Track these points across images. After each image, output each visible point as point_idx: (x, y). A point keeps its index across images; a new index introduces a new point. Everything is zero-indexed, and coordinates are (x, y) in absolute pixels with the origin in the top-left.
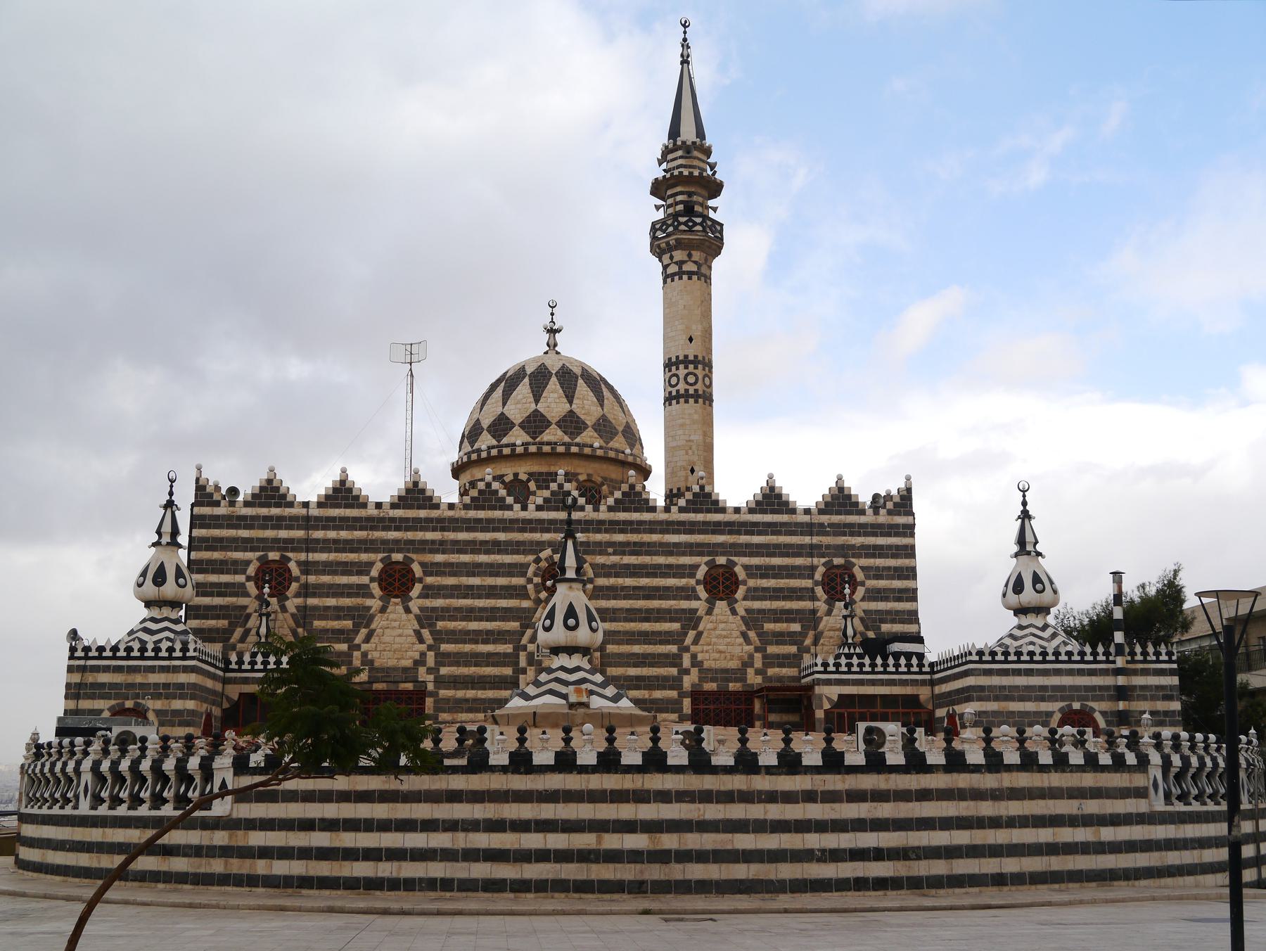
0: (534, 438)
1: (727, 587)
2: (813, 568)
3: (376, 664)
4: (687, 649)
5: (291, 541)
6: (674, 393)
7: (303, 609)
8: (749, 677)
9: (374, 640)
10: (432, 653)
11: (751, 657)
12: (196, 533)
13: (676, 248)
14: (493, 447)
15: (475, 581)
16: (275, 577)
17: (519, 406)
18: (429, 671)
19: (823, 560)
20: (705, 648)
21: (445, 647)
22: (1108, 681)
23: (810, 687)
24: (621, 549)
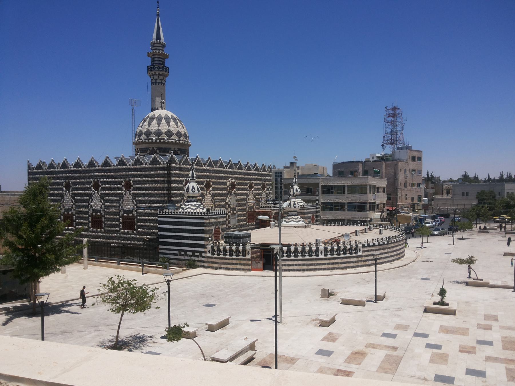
13: (161, 75)
22: (315, 210)
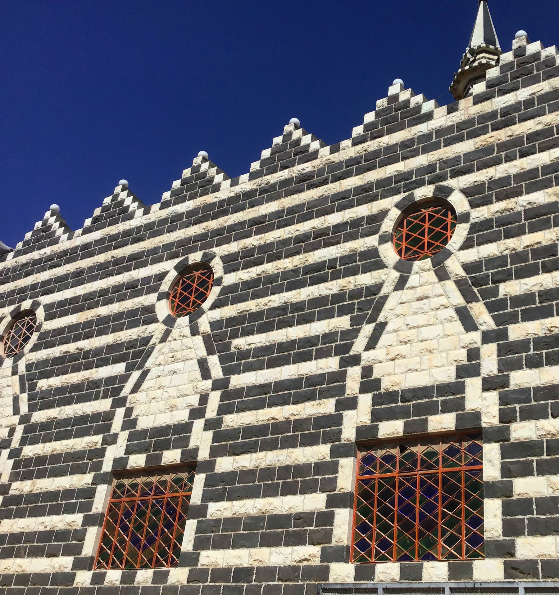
3: (386, 384)
9: (384, 339)
18: (489, 385)
21: (517, 332)
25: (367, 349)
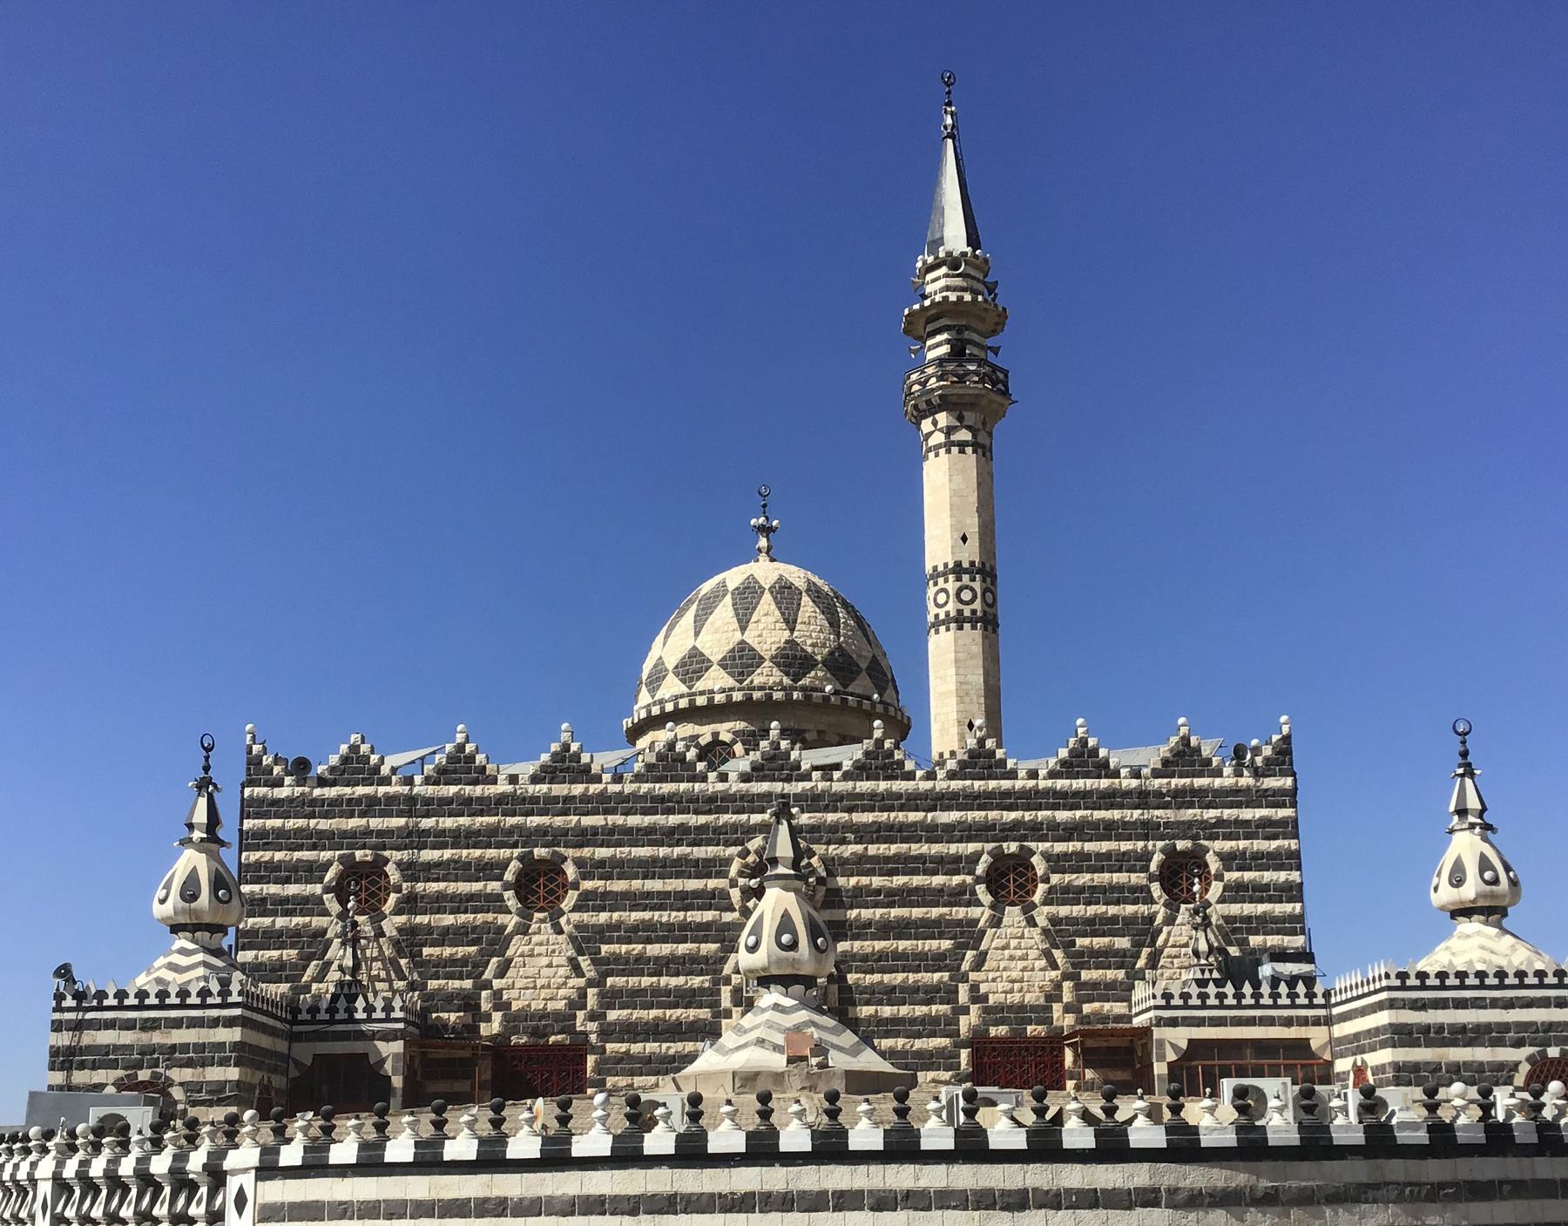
0: (741, 682)
1: (1021, 887)
2: (1146, 856)
4: (964, 978)
5: (388, 833)
6: (942, 617)
7: (409, 932)
8: (1055, 1015)
10: (595, 990)
11: (1058, 986)
12: (248, 824)
13: (940, 409)
14: (682, 696)
15: (655, 885)
16: (361, 883)
17: (718, 636)
18: (592, 1017)
19: (1160, 844)
20: (991, 975)
23: (1146, 1032)
24: (865, 834)
25: (496, 977)
